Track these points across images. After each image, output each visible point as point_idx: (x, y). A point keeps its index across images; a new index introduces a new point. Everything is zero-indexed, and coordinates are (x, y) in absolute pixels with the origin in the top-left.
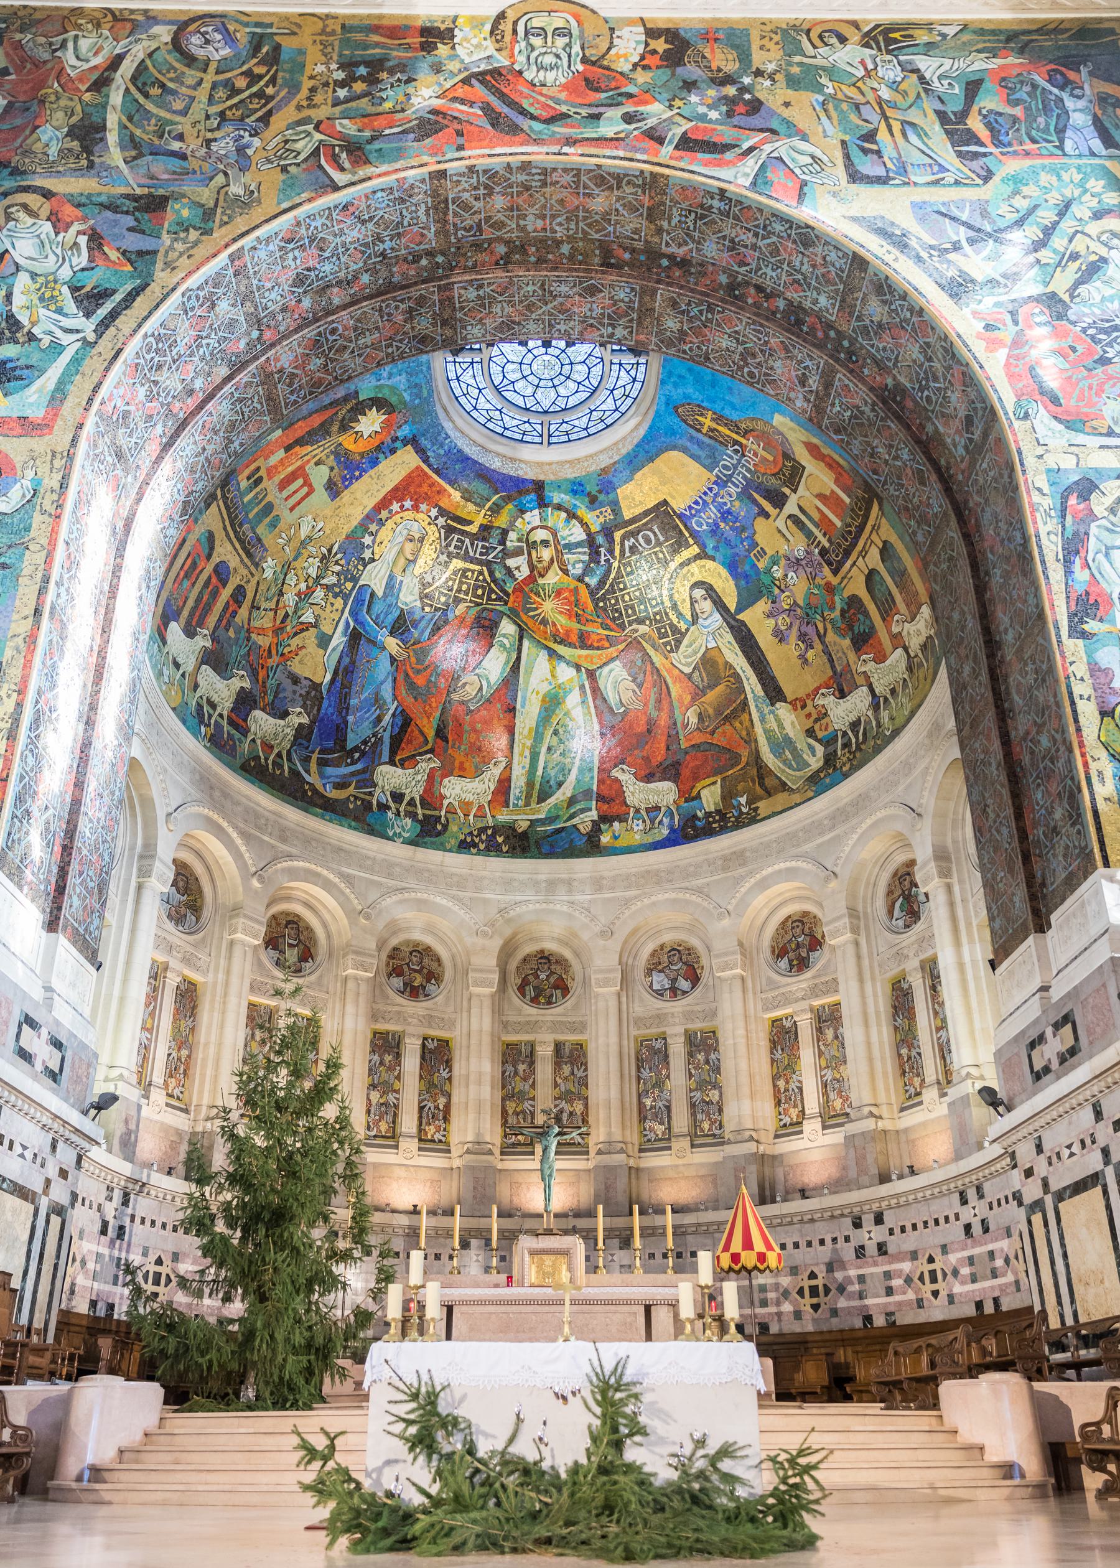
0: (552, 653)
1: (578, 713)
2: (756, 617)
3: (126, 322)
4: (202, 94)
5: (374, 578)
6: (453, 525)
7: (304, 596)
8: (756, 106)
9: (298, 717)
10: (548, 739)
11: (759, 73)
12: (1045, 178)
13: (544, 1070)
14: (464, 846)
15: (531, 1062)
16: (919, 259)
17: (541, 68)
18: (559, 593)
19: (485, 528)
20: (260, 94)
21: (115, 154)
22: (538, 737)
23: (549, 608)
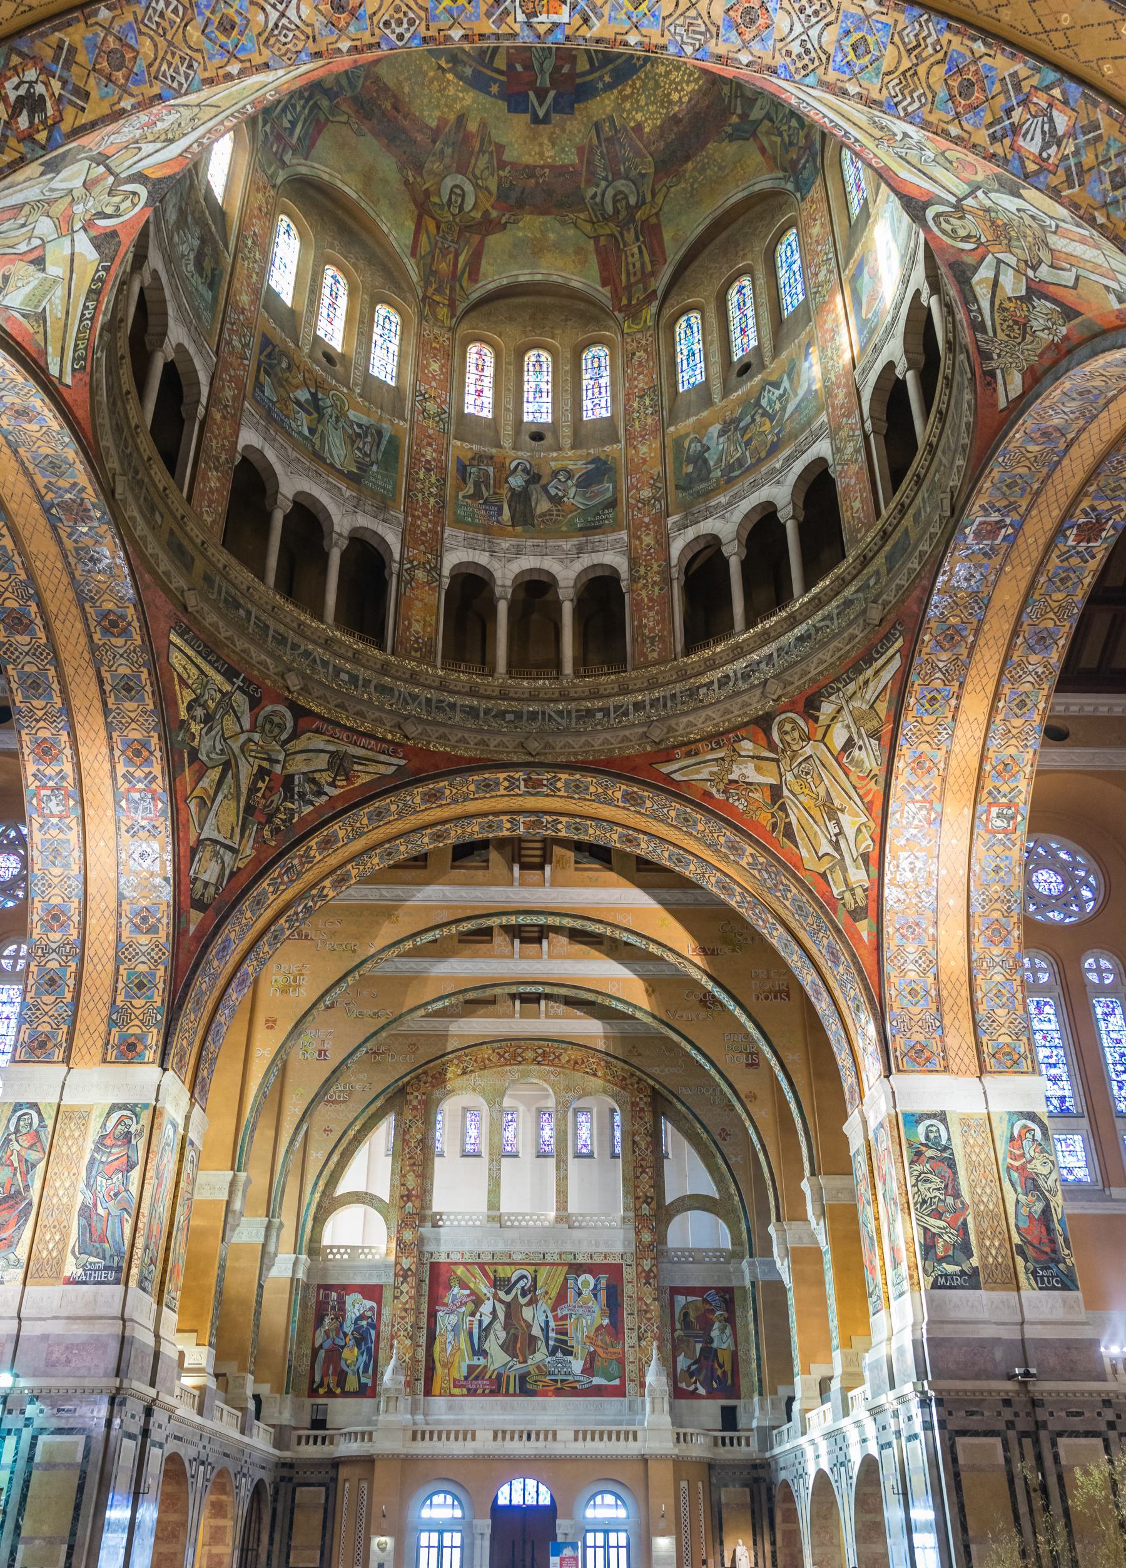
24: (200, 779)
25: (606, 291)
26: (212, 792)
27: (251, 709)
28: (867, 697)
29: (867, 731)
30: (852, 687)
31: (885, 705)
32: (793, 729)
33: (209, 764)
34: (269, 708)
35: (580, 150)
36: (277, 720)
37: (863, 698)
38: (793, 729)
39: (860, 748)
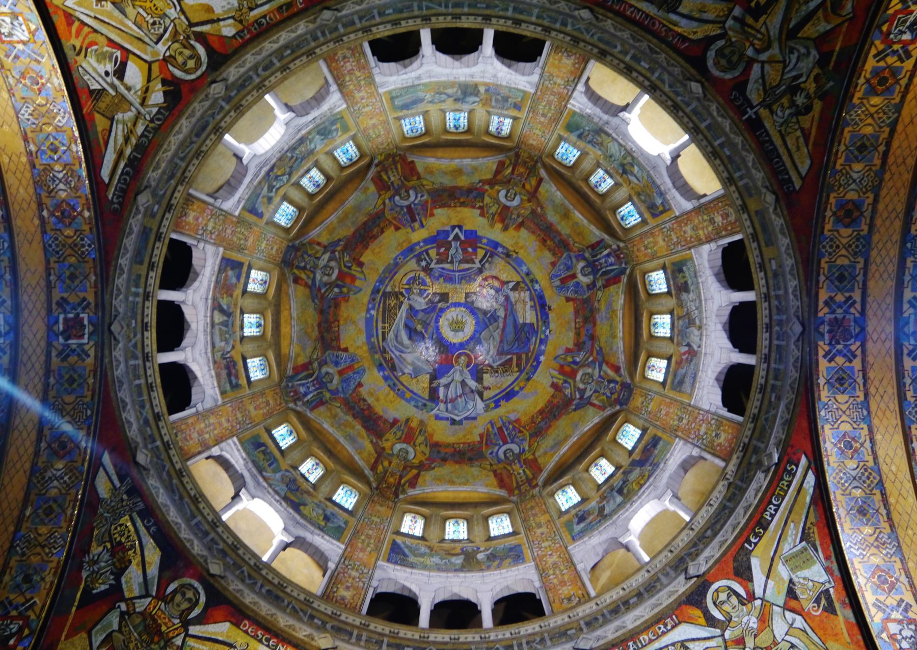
24: (827, 33)
25: (410, 160)
26: (820, 13)
27: (746, 82)
28: (120, 127)
29: (108, 94)
30: (140, 129)
31: (99, 129)
32: (185, 63)
33: (810, 44)
34: (728, 76)
35: (432, 215)
36: (723, 62)
37: (124, 123)
38: (185, 63)
39: (107, 74)
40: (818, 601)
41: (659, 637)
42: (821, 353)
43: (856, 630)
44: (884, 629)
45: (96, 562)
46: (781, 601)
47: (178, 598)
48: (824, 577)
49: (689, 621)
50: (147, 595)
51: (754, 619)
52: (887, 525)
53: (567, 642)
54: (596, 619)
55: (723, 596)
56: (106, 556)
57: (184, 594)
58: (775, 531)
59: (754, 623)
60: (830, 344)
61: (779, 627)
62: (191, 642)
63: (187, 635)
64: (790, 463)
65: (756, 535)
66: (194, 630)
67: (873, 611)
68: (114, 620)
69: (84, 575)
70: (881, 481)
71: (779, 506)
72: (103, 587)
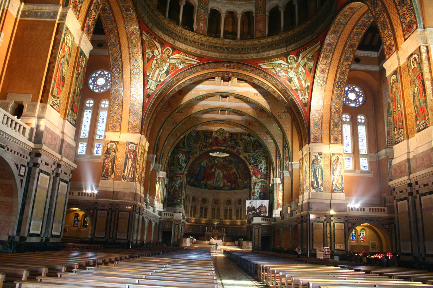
0: (219, 170)
1: (221, 175)
2: (238, 170)
3: (188, 164)
4: (193, 140)
5: (202, 164)
6: (210, 159)
7: (196, 168)
8: (237, 143)
9: (194, 178)
10: (218, 177)
11: (238, 139)
12: (259, 152)
13: (216, 211)
14: (209, 189)
15: (215, 210)
16: (248, 161)
17: (220, 137)
18: (220, 164)
19: (213, 160)
20: (197, 140)
21: (186, 147)
22: (217, 177)
23: (219, 165)
40: (309, 69)
41: (276, 61)
42: (333, 26)
43: (312, 78)
44: (317, 81)
45: (148, 53)
46: (303, 65)
47: (166, 52)
48: (312, 66)
49: (283, 60)
50: (160, 54)
51: (296, 66)
52: (330, 61)
53: (256, 53)
54: (264, 46)
55: (292, 58)
56: (149, 50)
57: (167, 51)
58: (308, 51)
59: (296, 66)
60: (336, 25)
61: (300, 70)
62: (171, 60)
63: (170, 59)
64: (317, 40)
65: (303, 50)
66: (170, 58)
67: (317, 77)
68: (155, 62)
69: (146, 56)
70: (334, 52)
71: (310, 47)
72: (151, 57)
